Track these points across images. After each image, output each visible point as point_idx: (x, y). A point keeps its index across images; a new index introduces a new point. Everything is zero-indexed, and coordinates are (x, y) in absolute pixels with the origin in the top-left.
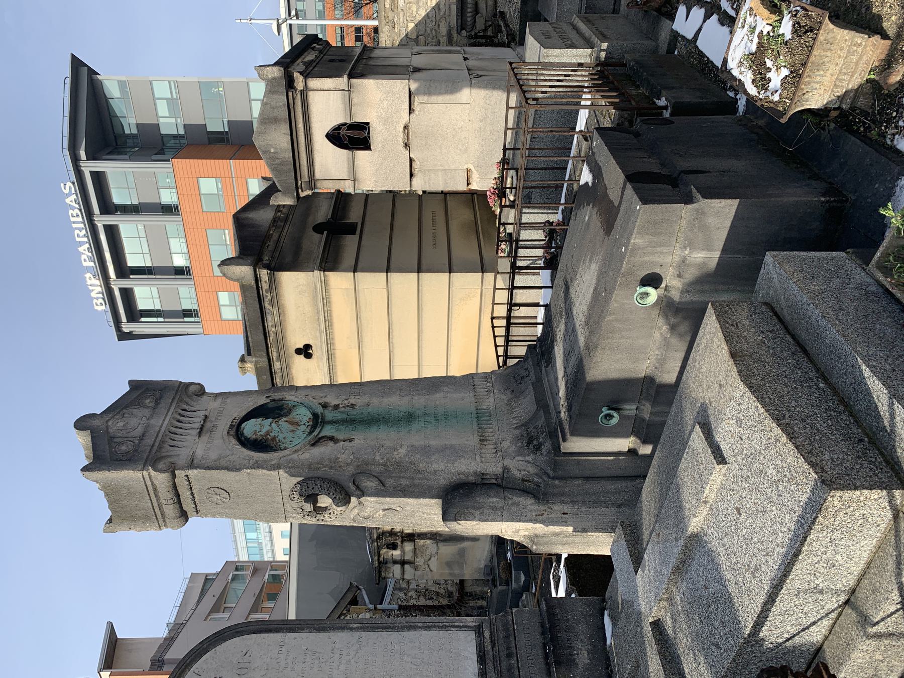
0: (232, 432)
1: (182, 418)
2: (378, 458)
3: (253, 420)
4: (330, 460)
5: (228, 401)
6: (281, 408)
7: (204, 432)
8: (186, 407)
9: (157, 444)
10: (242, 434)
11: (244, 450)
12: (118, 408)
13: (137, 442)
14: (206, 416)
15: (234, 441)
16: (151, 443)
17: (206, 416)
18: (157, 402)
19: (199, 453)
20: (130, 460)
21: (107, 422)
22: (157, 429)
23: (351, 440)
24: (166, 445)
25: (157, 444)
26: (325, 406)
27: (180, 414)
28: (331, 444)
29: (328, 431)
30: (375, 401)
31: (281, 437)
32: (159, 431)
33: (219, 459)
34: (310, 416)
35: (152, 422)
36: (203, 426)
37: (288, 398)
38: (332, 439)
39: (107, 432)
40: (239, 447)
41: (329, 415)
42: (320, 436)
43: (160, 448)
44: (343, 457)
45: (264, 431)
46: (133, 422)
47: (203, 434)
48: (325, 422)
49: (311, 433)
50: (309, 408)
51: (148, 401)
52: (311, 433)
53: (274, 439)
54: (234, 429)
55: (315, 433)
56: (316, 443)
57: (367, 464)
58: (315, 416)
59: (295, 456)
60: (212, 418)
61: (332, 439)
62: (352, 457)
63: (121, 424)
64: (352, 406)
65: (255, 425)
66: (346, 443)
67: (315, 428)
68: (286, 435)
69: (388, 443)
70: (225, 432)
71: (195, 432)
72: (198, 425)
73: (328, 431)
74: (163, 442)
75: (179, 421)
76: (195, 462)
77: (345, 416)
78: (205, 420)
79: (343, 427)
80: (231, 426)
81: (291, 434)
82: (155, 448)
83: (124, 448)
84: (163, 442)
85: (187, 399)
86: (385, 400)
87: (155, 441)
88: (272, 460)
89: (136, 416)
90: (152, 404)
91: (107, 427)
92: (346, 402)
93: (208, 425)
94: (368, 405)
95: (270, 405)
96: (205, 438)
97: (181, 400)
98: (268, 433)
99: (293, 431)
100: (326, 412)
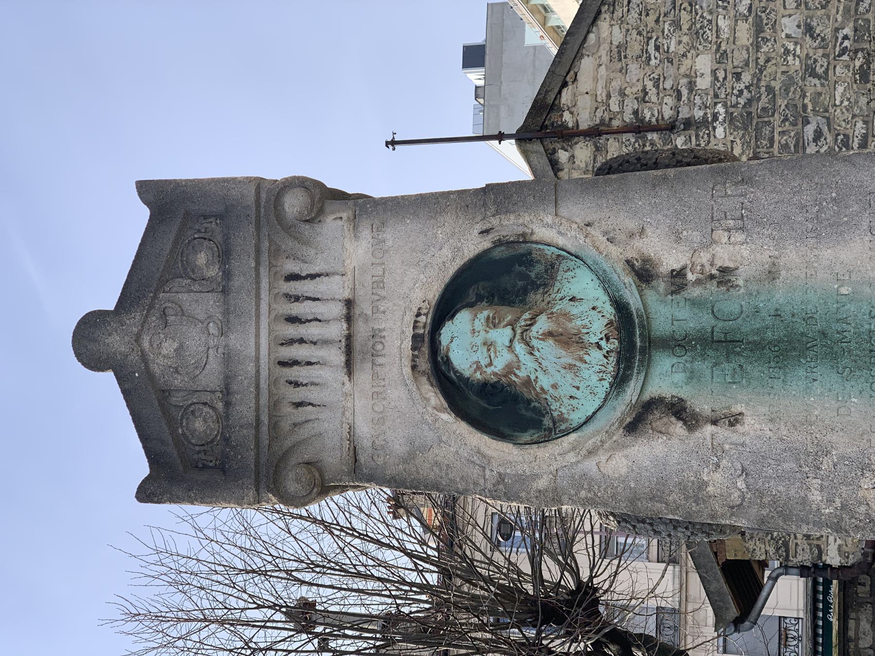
0: (424, 364)
1: (297, 309)
2: (816, 496)
3: (463, 318)
4: (682, 486)
5: (389, 236)
6: (526, 260)
7: (357, 356)
8: (292, 267)
9: (265, 418)
10: (448, 361)
11: (463, 428)
12: (143, 286)
13: (220, 405)
14: (349, 304)
15: (435, 398)
16: (251, 416)
17: (349, 304)
18: (225, 255)
19: (364, 430)
20: (222, 469)
21: (138, 338)
22: (251, 368)
23: (734, 420)
24: (287, 409)
25: (265, 418)
26: (644, 273)
27: (287, 296)
28: (678, 428)
29: (665, 378)
30: (792, 256)
31: (544, 382)
32: (258, 372)
33: (410, 457)
34: (609, 310)
35: (234, 340)
36: (349, 338)
37: (541, 233)
38: (678, 410)
39: (149, 375)
40: (447, 417)
41: (665, 314)
42: (646, 397)
43: (274, 426)
44: (717, 481)
45: (499, 365)
46: (195, 340)
47: (357, 366)
48: (655, 344)
49: (620, 382)
50: (605, 282)
51: (202, 259)
52: (620, 382)
53: (528, 383)
54: (426, 349)
55: (631, 393)
56: (636, 423)
57: (787, 518)
58: (620, 306)
59: (590, 465)
60: (364, 307)
61: (678, 410)
62: (741, 484)
63: (169, 347)
64: (724, 276)
65: (474, 348)
66: (722, 432)
67: (629, 367)
68: (557, 378)
69: (842, 444)
70: (407, 370)
71: (336, 356)
72: (337, 330)
73: (665, 378)
74: (275, 405)
75: (293, 320)
76: (362, 458)
77: (706, 321)
78: (349, 318)
79: (703, 367)
80: (417, 339)
81: (569, 376)
82: (264, 429)
83: (198, 425)
84: (274, 382)
85: (289, 244)
86: (827, 254)
87: (257, 409)
88: (536, 477)
89: (193, 319)
90: (213, 272)
91: (144, 356)
92: (704, 258)
93: (362, 330)
94: (772, 274)
95: (498, 254)
96: (363, 376)
97: (276, 252)
98: (510, 369)
99: (571, 367)
100: (651, 296)
